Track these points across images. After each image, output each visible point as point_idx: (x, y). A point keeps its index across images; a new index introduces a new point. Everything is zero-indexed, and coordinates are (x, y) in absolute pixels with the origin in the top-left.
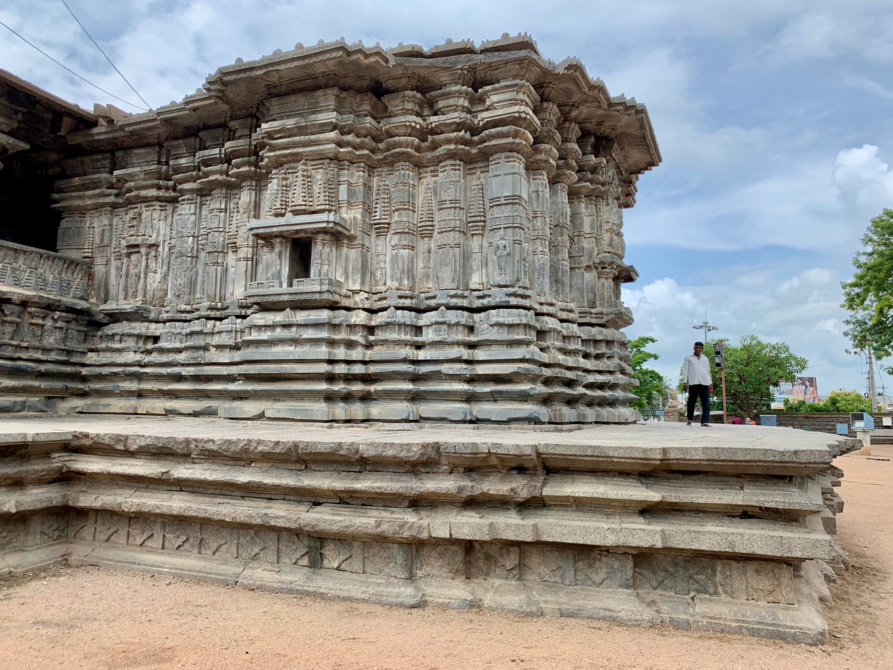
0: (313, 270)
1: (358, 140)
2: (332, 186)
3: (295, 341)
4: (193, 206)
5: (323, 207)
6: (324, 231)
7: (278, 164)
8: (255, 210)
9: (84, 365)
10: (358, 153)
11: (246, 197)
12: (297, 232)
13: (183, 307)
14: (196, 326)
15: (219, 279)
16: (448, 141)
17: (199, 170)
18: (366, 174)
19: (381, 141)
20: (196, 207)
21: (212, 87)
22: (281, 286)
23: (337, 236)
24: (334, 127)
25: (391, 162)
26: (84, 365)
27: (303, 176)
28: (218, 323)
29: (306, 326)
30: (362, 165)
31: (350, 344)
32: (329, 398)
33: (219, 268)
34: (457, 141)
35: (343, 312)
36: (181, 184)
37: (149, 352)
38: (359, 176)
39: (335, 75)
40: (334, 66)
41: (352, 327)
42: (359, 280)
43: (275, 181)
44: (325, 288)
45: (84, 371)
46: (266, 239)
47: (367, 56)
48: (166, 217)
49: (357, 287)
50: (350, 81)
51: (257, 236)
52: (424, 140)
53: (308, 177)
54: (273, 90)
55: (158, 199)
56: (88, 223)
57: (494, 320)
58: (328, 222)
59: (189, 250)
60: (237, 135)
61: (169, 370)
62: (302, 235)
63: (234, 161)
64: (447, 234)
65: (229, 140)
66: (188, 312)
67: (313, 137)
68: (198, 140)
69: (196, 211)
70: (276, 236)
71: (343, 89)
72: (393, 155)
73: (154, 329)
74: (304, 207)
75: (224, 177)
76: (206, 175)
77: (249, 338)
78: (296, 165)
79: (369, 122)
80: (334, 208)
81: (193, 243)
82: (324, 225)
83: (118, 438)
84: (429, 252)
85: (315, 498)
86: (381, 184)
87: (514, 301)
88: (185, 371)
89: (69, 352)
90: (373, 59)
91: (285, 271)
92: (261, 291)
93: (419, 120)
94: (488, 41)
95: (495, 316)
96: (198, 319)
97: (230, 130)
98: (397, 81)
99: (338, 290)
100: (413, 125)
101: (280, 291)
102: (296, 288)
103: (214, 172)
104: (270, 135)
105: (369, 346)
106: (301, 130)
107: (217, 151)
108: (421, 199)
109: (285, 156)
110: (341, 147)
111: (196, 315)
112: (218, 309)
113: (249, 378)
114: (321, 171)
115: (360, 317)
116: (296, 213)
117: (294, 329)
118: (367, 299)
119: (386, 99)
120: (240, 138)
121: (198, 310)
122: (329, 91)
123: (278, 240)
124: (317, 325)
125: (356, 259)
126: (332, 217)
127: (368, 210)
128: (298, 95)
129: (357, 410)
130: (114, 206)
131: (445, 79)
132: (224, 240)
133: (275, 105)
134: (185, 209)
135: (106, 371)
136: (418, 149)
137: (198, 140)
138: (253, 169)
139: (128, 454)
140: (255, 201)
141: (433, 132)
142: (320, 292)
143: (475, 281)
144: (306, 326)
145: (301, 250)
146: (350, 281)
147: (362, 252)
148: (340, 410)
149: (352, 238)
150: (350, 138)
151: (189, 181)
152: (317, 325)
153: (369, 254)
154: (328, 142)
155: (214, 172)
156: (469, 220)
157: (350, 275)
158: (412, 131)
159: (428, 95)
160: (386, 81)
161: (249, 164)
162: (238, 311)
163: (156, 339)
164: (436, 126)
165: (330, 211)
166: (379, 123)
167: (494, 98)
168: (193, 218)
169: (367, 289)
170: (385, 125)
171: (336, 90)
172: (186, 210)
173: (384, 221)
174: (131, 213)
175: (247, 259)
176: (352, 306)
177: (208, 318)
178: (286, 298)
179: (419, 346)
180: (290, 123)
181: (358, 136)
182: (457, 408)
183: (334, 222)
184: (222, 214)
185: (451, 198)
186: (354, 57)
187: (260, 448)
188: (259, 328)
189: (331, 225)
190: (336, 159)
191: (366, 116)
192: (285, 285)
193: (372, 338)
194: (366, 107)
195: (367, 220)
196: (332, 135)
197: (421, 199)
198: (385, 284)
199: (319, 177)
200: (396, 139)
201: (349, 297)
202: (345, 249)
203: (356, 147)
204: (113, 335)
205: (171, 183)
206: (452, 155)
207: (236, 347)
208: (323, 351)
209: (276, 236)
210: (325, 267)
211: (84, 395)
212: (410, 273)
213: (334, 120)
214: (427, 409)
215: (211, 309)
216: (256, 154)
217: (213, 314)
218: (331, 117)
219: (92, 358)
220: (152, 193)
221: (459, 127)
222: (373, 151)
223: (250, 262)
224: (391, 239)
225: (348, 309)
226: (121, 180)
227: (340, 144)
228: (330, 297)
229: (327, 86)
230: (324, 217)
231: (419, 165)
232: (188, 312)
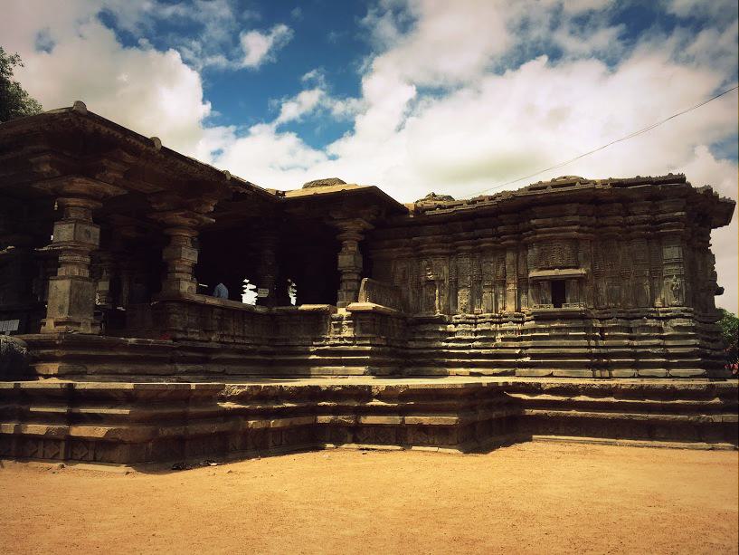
2: (575, 253)
3: (566, 337)
7: (539, 242)
9: (407, 348)
13: (470, 316)
14: (485, 327)
16: (639, 229)
23: (580, 280)
26: (407, 348)
32: (587, 366)
34: (646, 230)
37: (448, 341)
45: (410, 352)
46: (537, 282)
55: (441, 254)
56: (393, 268)
57: (675, 324)
61: (472, 351)
71: (581, 203)
73: (451, 328)
79: (594, 220)
83: (539, 385)
85: (649, 409)
87: (687, 315)
88: (483, 351)
89: (403, 341)
95: (676, 323)
105: (603, 338)
113: (533, 356)
129: (606, 373)
130: (409, 257)
135: (425, 351)
139: (542, 392)
141: (630, 224)
143: (658, 303)
148: (598, 373)
150: (586, 228)
154: (573, 230)
158: (620, 225)
163: (452, 334)
167: (666, 207)
174: (425, 263)
179: (631, 338)
182: (662, 371)
187: (623, 387)
188: (541, 330)
190: (576, 241)
196: (576, 227)
204: (425, 332)
206: (642, 237)
208: (584, 342)
211: (409, 365)
212: (619, 298)
214: (644, 372)
215: (492, 317)
219: (412, 344)
220: (440, 251)
221: (645, 222)
226: (418, 243)
231: (619, 240)
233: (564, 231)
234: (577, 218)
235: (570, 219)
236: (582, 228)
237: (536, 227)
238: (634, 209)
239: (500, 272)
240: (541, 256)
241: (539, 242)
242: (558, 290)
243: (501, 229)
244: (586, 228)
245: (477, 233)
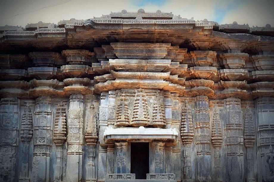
7: (117, 89)
38: (176, 103)
50: (174, 39)
64: (235, 146)
67: (151, 74)
72: (198, 91)
75: (52, 89)
81: (16, 136)
94: (257, 27)
106: (140, 69)
107: (51, 69)
109: (127, 84)
119: (193, 54)
122: (164, 45)
125: (176, 160)
131: (232, 46)
133: (118, 47)
150: (176, 77)
154: (160, 78)
156: (246, 137)
160: (194, 42)
171: (169, 46)
173: (191, 134)
175: (79, 154)
185: (236, 123)
190: (163, 92)
194: (181, 57)
196: (166, 75)
198: (191, 178)
213: (169, 65)
221: (241, 78)
224: (194, 146)
231: (210, 98)
233: (151, 78)
234: (167, 63)
235: (160, 63)
237: (114, 69)
238: (229, 62)
239: (60, 128)
240: (119, 109)
241: (117, 89)
243: (66, 68)
244: (176, 77)
245: (32, 71)
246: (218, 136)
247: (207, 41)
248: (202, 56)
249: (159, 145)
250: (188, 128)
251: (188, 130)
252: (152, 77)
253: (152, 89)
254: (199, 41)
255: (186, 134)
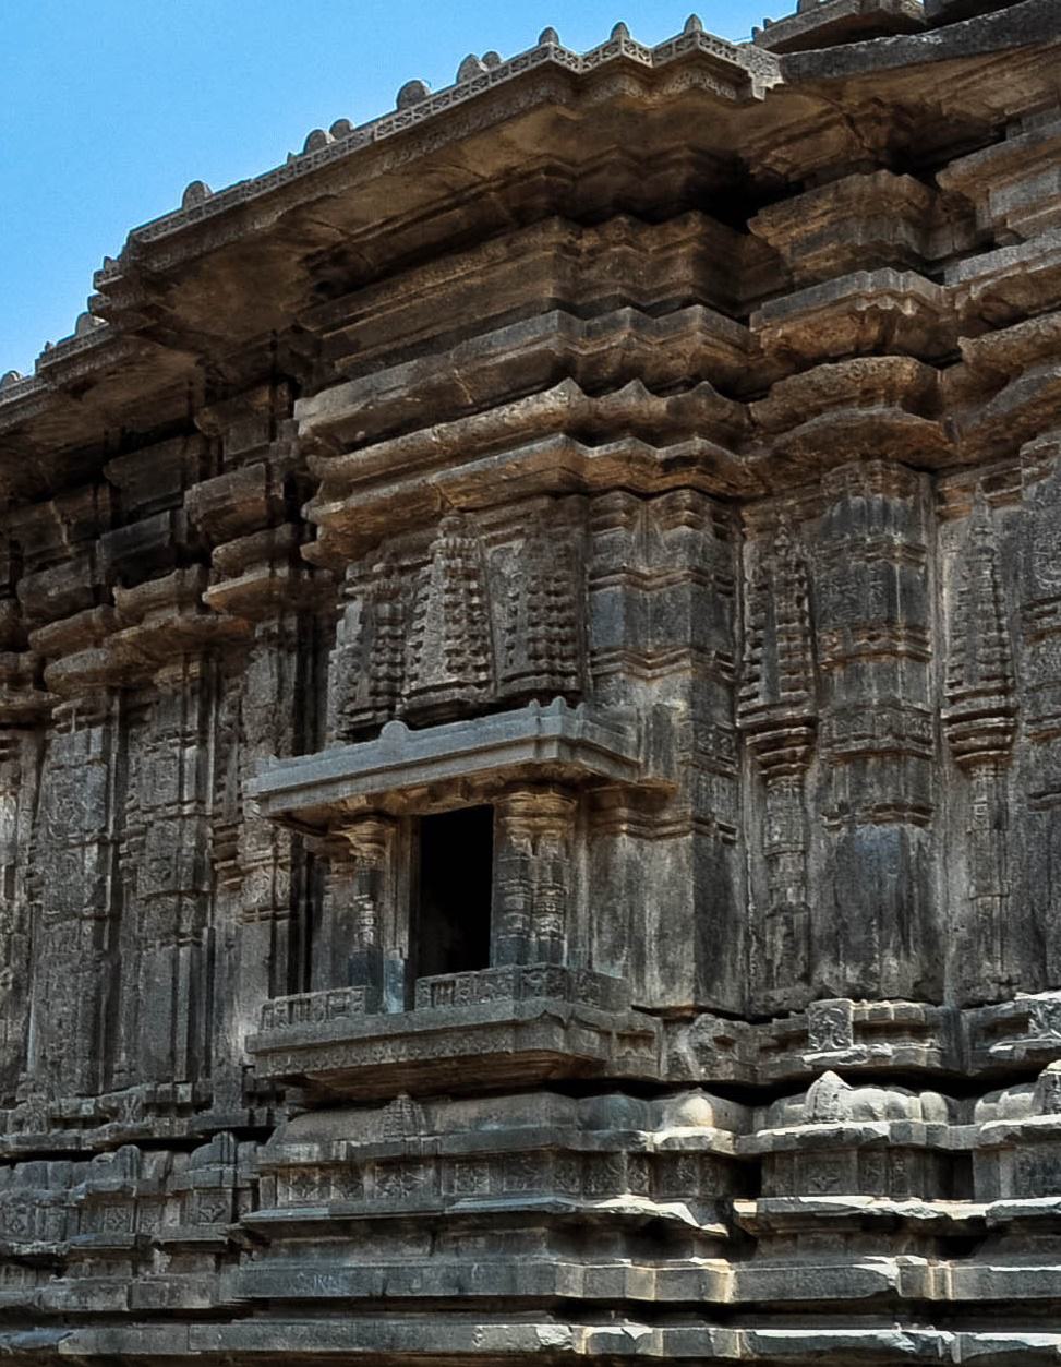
0: (501, 937)
1: (660, 405)
3: (433, 1228)
4: (97, 732)
5: (527, 684)
6: (535, 779)
8: (299, 727)
10: (661, 453)
11: (263, 679)
12: (435, 791)
15: (183, 995)
17: (111, 601)
18: (706, 535)
19: (762, 392)
20: (107, 734)
21: (119, 304)
22: (374, 1005)
24: (557, 371)
25: (804, 470)
27: (450, 572)
28: (181, 1160)
29: (471, 1161)
30: (686, 496)
31: (656, 1238)
33: (183, 953)
35: (621, 1100)
36: (57, 656)
39: (550, 170)
40: (539, 142)
41: (663, 1169)
42: (689, 968)
43: (355, 608)
44: (537, 1004)
47: (651, 79)
48: (16, 781)
49: (682, 998)
51: (288, 818)
52: (950, 358)
53: (469, 576)
54: (331, 272)
58: (540, 743)
59: (88, 892)
60: (229, 453)
62: (455, 800)
63: (219, 550)
65: (204, 476)
66: (88, 1123)
68: (104, 495)
69: (106, 754)
70: (360, 817)
74: (457, 693)
76: (135, 616)
77: (266, 1214)
78: (424, 534)
79: (696, 333)
80: (572, 683)
82: (526, 755)
84: (999, 823)
86: (772, 563)
90: (676, 87)
91: (397, 951)
92: (303, 1030)
93: (917, 284)
96: (113, 1147)
97: (207, 440)
98: (805, 145)
99: (592, 1011)
100: (889, 304)
101: (369, 1025)
102: (431, 1013)
103: (160, 603)
104: (338, 438)
108: (947, 598)
110: (592, 441)
111: (105, 1133)
112: (182, 1110)
114: (517, 544)
115: (697, 1121)
116: (421, 717)
117: (424, 1177)
118: (724, 1043)
120: (237, 461)
121: (115, 1113)
123: (366, 828)
124: (511, 1160)
125: (673, 882)
126: (553, 719)
127: (720, 678)
128: (417, 275)
132: (200, 849)
134: (71, 746)
136: (924, 401)
137: (104, 495)
138: (283, 572)
140: (300, 693)
142: (515, 1026)
144: (471, 1161)
145: (452, 871)
146: (653, 975)
147: (696, 848)
149: (648, 801)
150: (630, 399)
151: (83, 644)
152: (511, 1160)
153: (733, 855)
155: (160, 603)
157: (652, 947)
159: (942, 180)
160: (764, 153)
161: (273, 556)
162: (239, 1113)
164: (988, 296)
165: (545, 697)
166: (745, 321)
168: (96, 776)
169: (730, 1001)
170: (770, 331)
172: (79, 748)
176: (661, 1073)
177: (148, 1144)
178: (388, 1055)
180: (396, 383)
181: (658, 387)
183: (563, 741)
184: (190, 752)
186: (601, 96)
189: (551, 753)
191: (688, 302)
192: (395, 1006)
193: (745, 1207)
195: (720, 713)
197: (947, 598)
199: (509, 569)
200: (818, 374)
201: (645, 1038)
202: (625, 845)
203: (652, 433)
205: (25, 661)
207: (227, 1253)
209: (360, 817)
210: (548, 923)
216: (293, 515)
217: (162, 1126)
218: (541, 336)
222: (733, 438)
223: (283, 924)
225: (649, 1089)
227: (586, 432)
228: (559, 1042)
229: (524, 219)
230: (523, 721)
232: (88, 1123)
236: (603, 404)
242: (452, 871)
244: (630, 399)
246: (977, 694)
247: (828, 125)
248: (814, 226)
249: (520, 806)
250: (772, 681)
251: (773, 692)
252: (493, 433)
253: (519, 499)
254: (791, 140)
255: (762, 717)
